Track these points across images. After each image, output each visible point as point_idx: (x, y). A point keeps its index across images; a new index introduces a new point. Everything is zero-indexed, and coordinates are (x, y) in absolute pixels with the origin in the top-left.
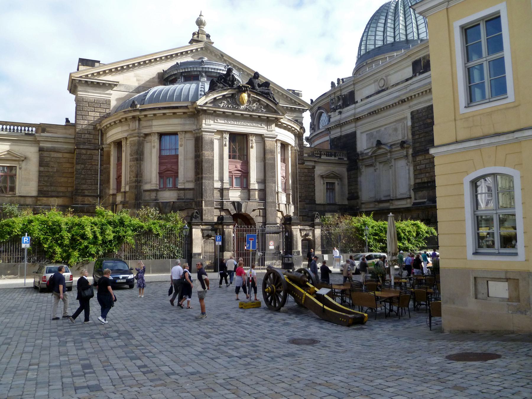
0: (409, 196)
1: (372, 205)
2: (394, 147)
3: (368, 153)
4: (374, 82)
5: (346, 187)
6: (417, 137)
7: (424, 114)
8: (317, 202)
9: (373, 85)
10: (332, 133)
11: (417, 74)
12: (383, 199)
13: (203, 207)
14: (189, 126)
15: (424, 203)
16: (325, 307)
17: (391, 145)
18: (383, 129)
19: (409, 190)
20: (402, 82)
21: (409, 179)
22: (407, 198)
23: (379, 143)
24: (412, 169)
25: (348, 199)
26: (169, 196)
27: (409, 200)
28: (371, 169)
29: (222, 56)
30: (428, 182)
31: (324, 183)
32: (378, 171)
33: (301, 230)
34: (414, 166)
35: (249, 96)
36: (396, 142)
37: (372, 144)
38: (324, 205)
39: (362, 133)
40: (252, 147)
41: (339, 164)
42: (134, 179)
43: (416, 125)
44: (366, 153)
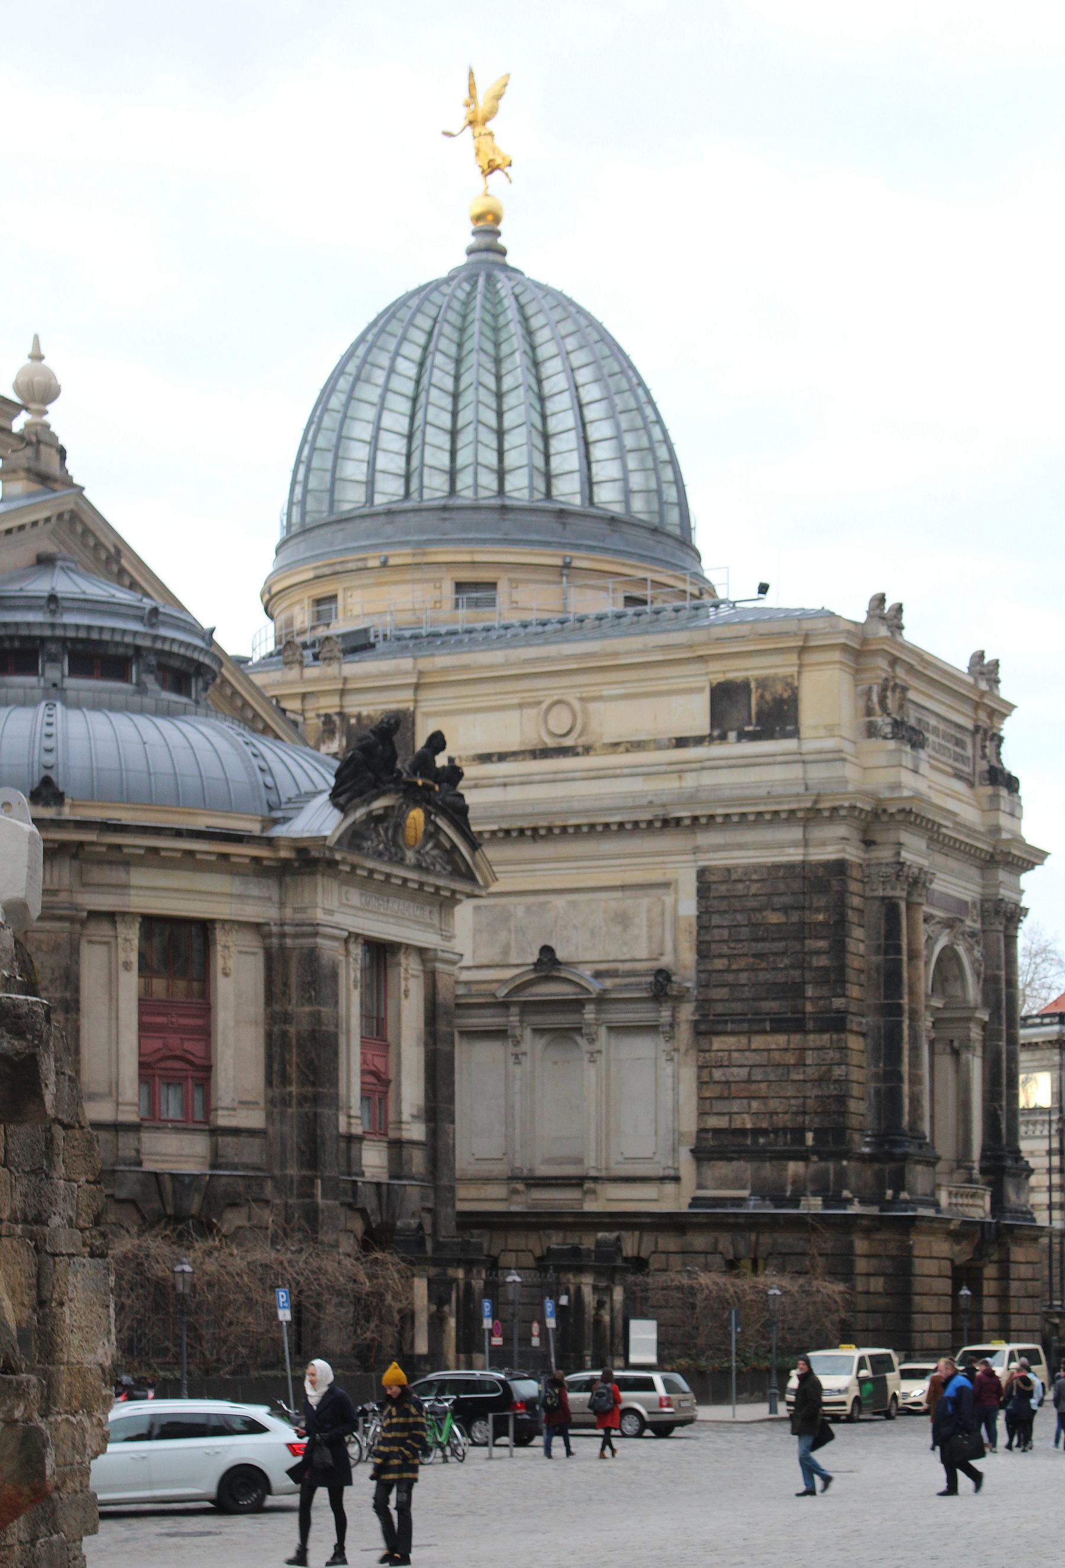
0: (671, 1172)
2: (608, 983)
4: (521, 706)
6: (719, 964)
7: (754, 888)
9: (514, 716)
11: (732, 735)
12: (543, 1170)
13: (320, 1200)
15: (739, 1202)
19: (674, 1150)
23: (548, 961)
27: (670, 1188)
29: (118, 552)
30: (757, 1132)
34: (701, 1068)
35: (428, 820)
36: (621, 967)
40: (406, 992)
43: (716, 920)
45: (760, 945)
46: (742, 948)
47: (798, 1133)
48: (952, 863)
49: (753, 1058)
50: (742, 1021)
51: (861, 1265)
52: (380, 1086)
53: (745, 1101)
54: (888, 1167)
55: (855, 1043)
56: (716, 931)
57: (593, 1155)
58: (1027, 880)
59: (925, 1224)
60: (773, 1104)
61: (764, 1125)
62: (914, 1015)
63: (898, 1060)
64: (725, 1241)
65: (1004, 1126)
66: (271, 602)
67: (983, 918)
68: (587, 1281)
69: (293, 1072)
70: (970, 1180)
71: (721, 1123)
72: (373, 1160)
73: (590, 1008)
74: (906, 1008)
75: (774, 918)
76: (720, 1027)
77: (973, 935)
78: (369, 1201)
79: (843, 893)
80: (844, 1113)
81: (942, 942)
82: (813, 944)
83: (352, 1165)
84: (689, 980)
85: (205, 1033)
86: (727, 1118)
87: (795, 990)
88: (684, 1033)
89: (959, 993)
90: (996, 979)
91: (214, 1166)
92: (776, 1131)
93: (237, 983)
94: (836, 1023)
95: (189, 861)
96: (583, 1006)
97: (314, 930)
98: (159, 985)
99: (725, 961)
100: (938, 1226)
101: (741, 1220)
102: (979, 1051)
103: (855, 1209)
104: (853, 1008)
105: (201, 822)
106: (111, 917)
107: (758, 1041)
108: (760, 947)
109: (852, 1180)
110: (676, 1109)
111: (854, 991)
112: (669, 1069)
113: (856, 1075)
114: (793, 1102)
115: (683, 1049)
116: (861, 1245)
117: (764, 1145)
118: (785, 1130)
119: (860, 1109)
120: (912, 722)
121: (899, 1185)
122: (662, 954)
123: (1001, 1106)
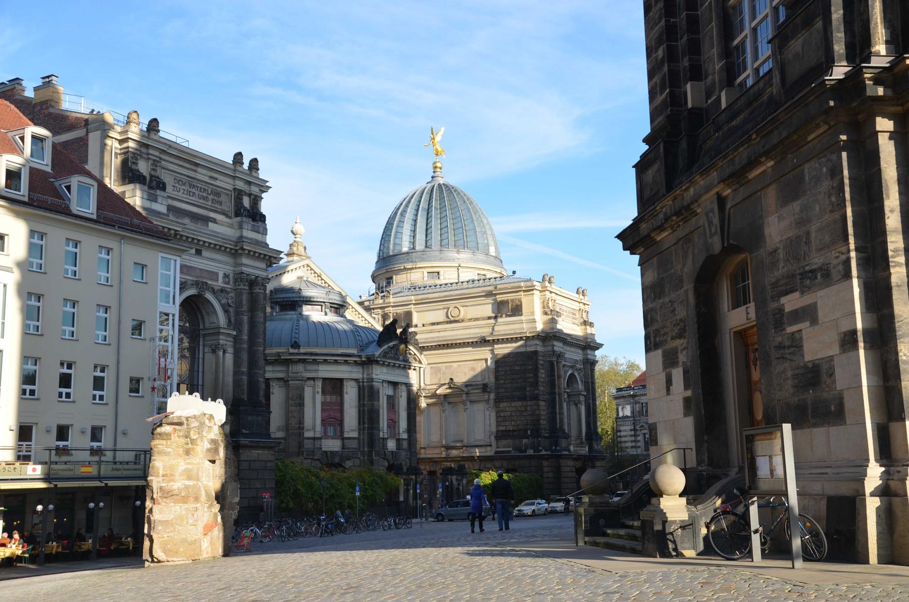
6: (502, 382)
14: (356, 373)
15: (509, 452)
18: (455, 365)
20: (483, 319)
22: (486, 446)
24: (493, 414)
26: (332, 445)
27: (489, 448)
30: (514, 431)
32: (446, 412)
37: (440, 380)
42: (297, 426)
47: (526, 430)
48: (572, 349)
51: (546, 469)
52: (393, 423)
55: (542, 403)
58: (597, 353)
62: (560, 395)
63: (555, 408)
64: (505, 463)
66: (374, 278)
68: (454, 477)
69: (366, 420)
70: (582, 443)
71: (504, 428)
72: (391, 445)
75: (517, 368)
78: (390, 457)
79: (537, 360)
81: (570, 372)
83: (384, 446)
85: (342, 411)
88: (492, 402)
91: (343, 448)
93: (351, 395)
94: (536, 398)
95: (336, 362)
97: (372, 380)
98: (328, 398)
100: (570, 457)
103: (544, 453)
105: (340, 351)
106: (313, 379)
107: (513, 404)
108: (514, 376)
110: (490, 425)
111: (541, 388)
112: (488, 413)
113: (542, 413)
116: (545, 463)
120: (558, 310)
121: (557, 444)
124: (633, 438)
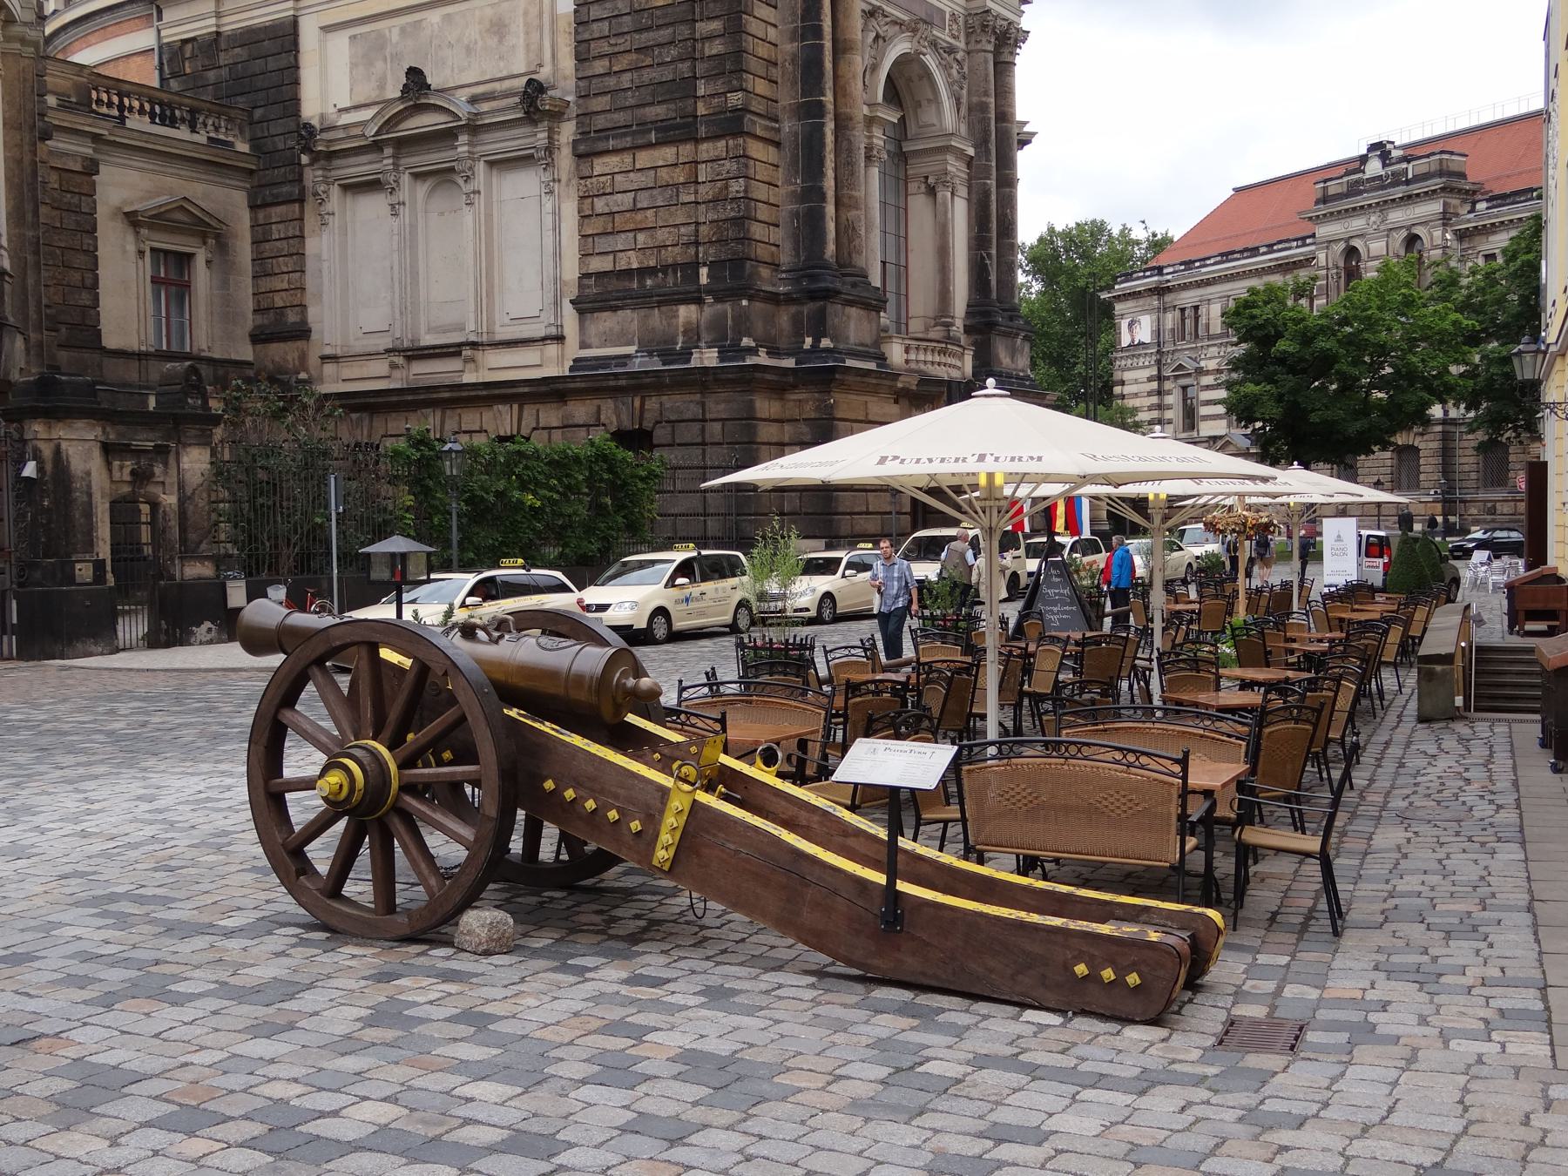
0: (553, 331)
1: (380, 367)
2: (485, 107)
3: (364, 124)
5: (248, 280)
6: (600, 67)
8: (111, 341)
10: (168, 15)
12: (428, 340)
16: (902, 886)
17: (473, 100)
19: (557, 303)
21: (558, 254)
22: (544, 339)
24: (570, 210)
25: (258, 338)
27: (552, 349)
28: (372, 207)
30: (643, 272)
31: (141, 253)
32: (405, 212)
33: (109, 450)
36: (497, 86)
37: (382, 87)
38: (140, 356)
39: (327, 29)
41: (215, 164)
44: (345, 127)
45: (645, 36)
46: (623, 43)
49: (638, 180)
50: (625, 135)
53: (631, 235)
54: (807, 309)
56: (595, 26)
57: (472, 316)
59: (850, 378)
60: (662, 236)
61: (652, 263)
62: (842, 123)
63: (821, 174)
65: (993, 278)
67: (968, 35)
70: (949, 339)
73: (463, 138)
74: (830, 107)
76: (601, 146)
77: (951, 50)
80: (746, 239)
81: (900, 47)
82: (704, 28)
84: (568, 93)
86: (611, 257)
87: (684, 88)
89: (935, 121)
90: (983, 107)
92: (665, 269)
96: (456, 138)
99: (606, 62)
101: (623, 382)
102: (963, 191)
103: (762, 359)
104: (757, 106)
107: (644, 158)
109: (759, 327)
113: (761, 192)
114: (683, 230)
115: (564, 178)
116: (765, 406)
117: (653, 287)
118: (675, 266)
119: (772, 238)
122: (540, 65)
123: (989, 255)
124: (1154, 400)
